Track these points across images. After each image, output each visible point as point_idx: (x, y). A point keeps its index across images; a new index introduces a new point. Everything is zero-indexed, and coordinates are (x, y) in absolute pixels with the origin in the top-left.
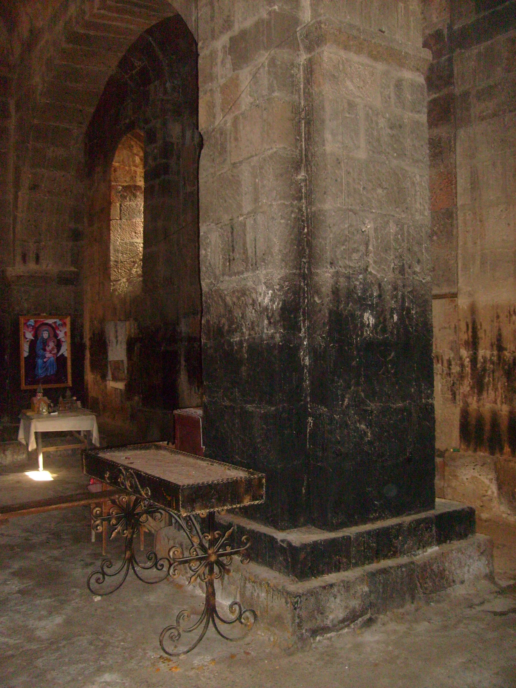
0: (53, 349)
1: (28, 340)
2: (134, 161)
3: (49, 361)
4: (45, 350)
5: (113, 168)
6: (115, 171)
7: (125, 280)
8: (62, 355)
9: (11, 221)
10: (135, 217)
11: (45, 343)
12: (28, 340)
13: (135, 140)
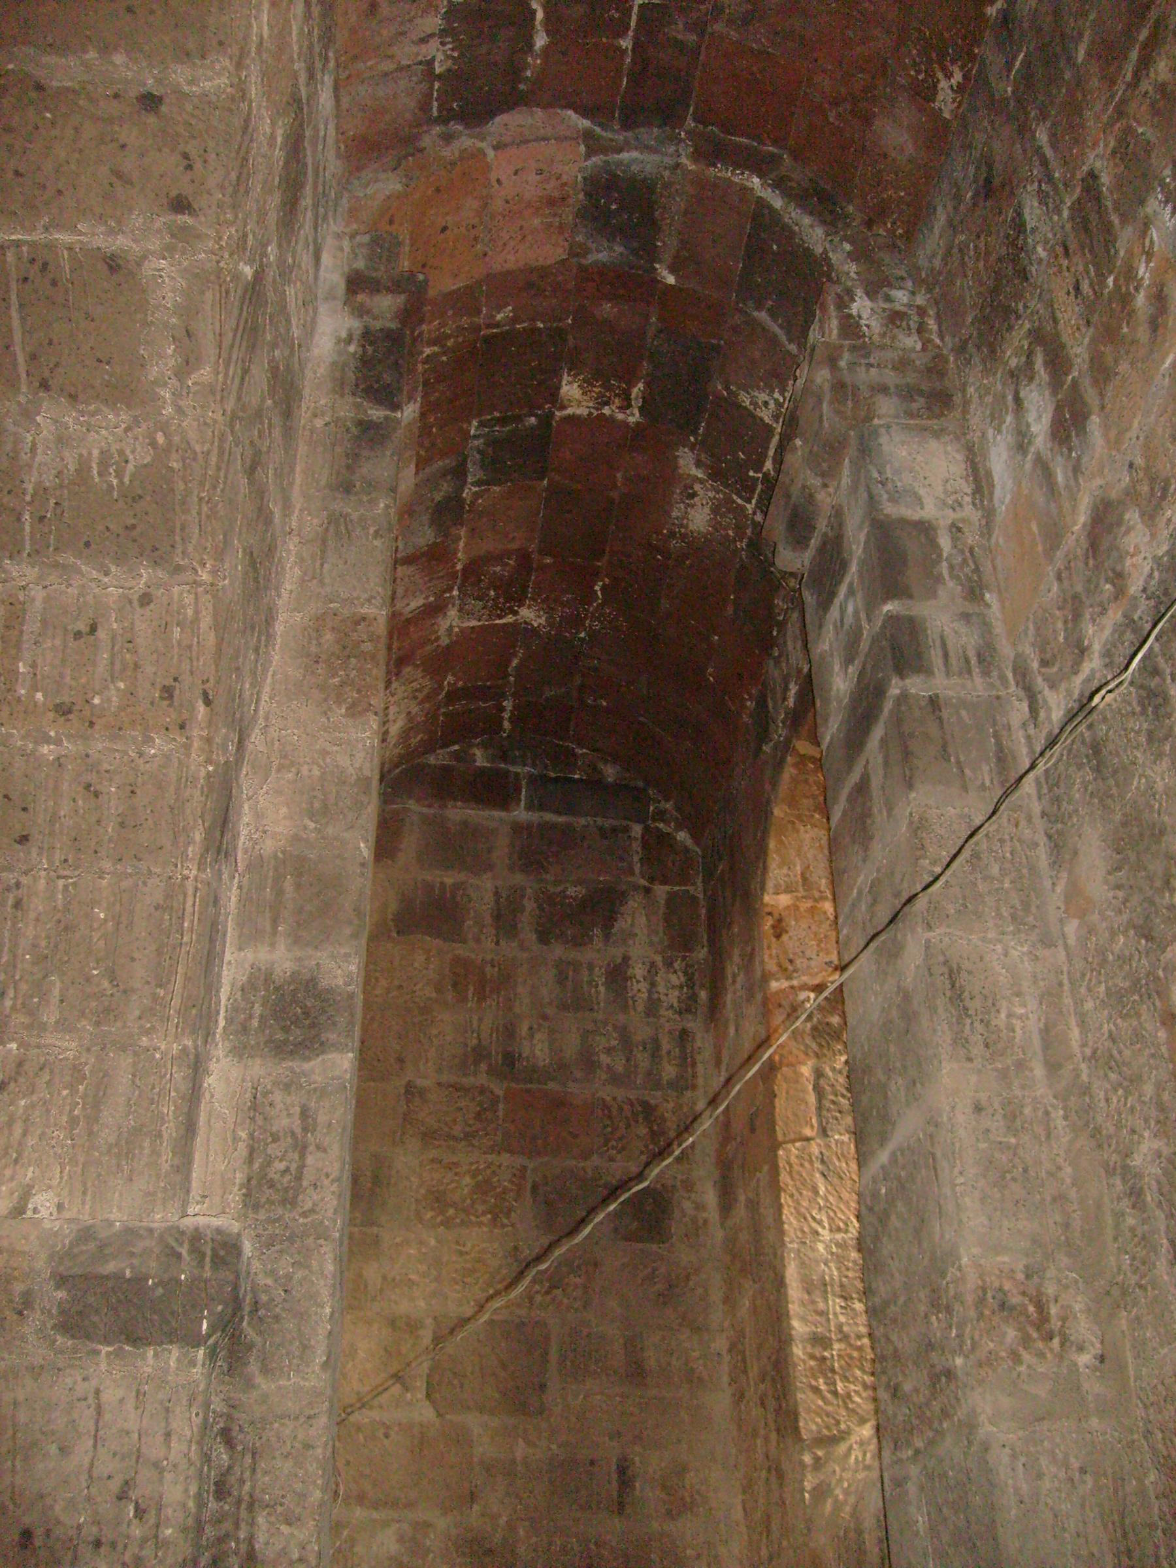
5: (768, 923)
6: (779, 930)
7: (867, 1431)
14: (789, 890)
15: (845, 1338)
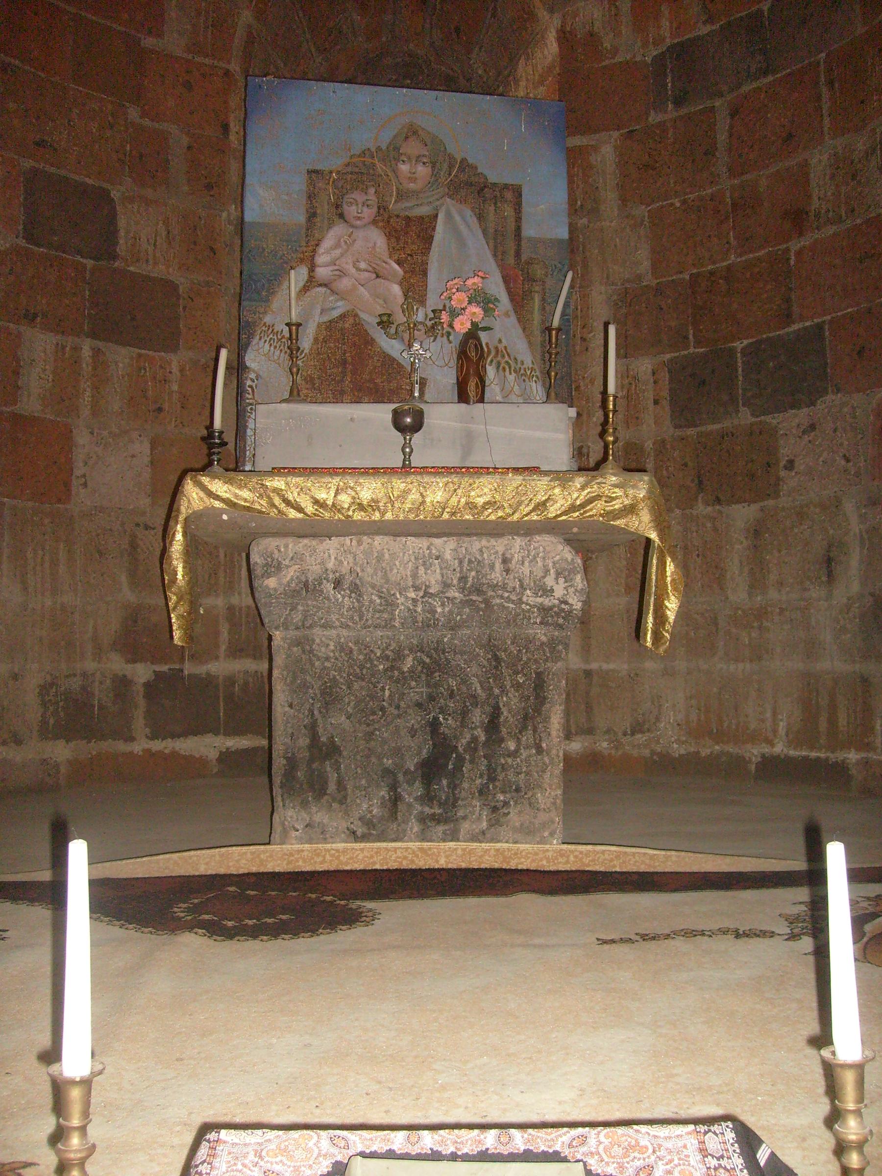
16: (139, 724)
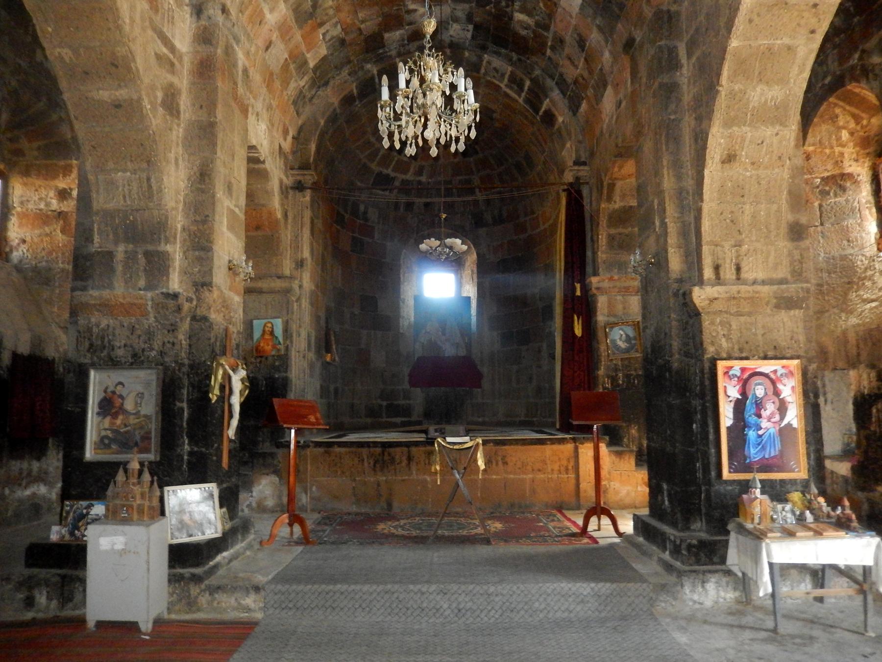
0: (772, 414)
1: (731, 399)
2: (839, 139)
3: (767, 434)
4: (759, 416)
8: (789, 425)
9: (692, 220)
10: (845, 219)
11: (759, 405)
12: (731, 399)
13: (841, 103)
14: (813, 145)
15: (828, 284)
16: (384, 415)
